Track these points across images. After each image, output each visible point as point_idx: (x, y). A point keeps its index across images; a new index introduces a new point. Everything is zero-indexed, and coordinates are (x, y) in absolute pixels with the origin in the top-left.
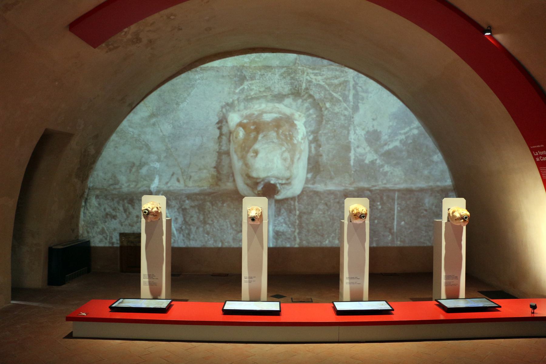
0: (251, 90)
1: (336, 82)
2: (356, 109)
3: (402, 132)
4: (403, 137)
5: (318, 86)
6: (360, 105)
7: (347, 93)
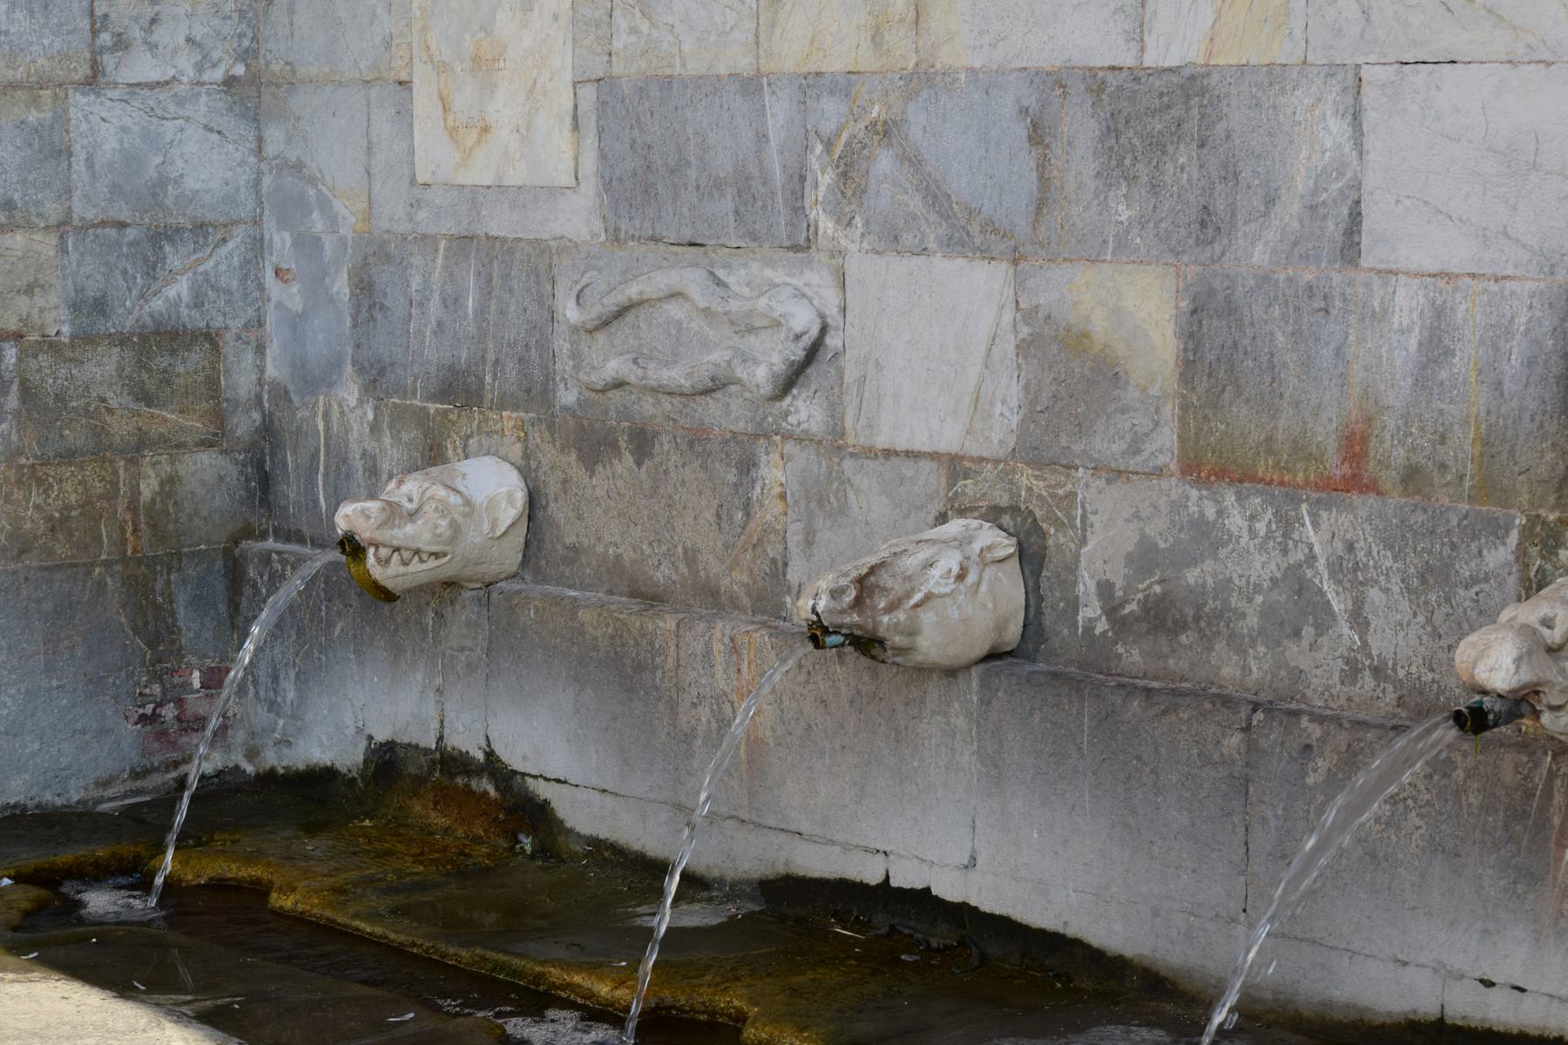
0: (966, 495)
1: (1060, 492)
2: (1083, 541)
3: (1140, 587)
4: (1140, 596)
5: (1040, 496)
6: (1088, 534)
7: (1073, 512)
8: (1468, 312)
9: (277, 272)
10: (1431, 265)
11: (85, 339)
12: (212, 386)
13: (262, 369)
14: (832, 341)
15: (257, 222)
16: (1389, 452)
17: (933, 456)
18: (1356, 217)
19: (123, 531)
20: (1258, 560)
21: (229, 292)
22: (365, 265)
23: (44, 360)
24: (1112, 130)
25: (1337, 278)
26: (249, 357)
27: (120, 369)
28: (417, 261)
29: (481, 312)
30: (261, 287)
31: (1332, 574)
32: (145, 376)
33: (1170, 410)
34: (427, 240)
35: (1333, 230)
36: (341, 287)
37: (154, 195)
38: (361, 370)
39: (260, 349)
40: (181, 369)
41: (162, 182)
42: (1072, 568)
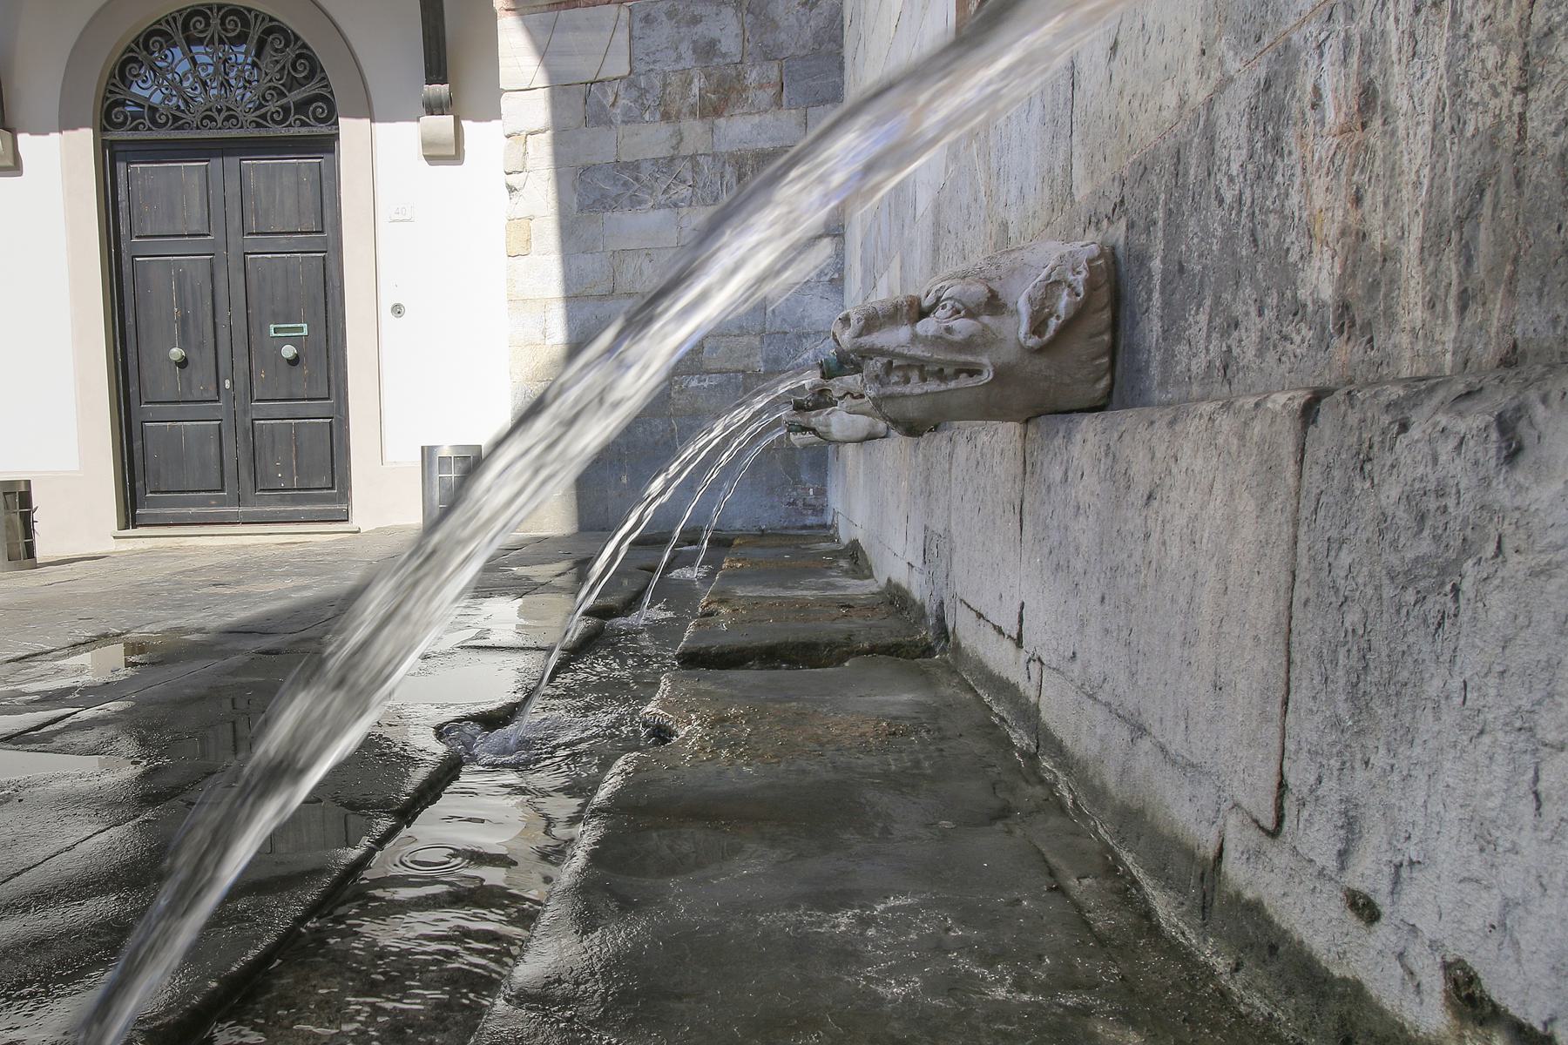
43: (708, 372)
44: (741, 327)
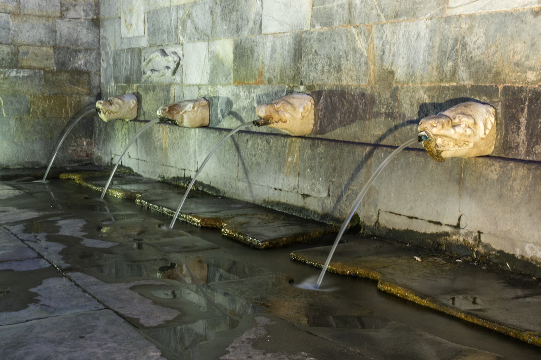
8: (279, 42)
9: (103, 60)
10: (273, 32)
11: (59, 71)
12: (89, 83)
13: (100, 80)
14: (181, 63)
15: (99, 49)
16: (267, 75)
17: (196, 85)
18: (261, 24)
19: (68, 111)
20: (245, 101)
21: (92, 64)
22: (115, 56)
23: (50, 75)
24: (223, 10)
25: (258, 37)
26: (97, 77)
27: (67, 77)
28: (122, 54)
29: (131, 64)
30: (100, 63)
31: (257, 103)
32: (73, 80)
33: (232, 70)
34: (123, 50)
35: (258, 26)
36: (111, 61)
37: (75, 42)
38: (114, 78)
39: (100, 76)
40: (82, 79)
41: (77, 40)
42: (217, 107)
43: (22, 68)
44: (41, 42)
